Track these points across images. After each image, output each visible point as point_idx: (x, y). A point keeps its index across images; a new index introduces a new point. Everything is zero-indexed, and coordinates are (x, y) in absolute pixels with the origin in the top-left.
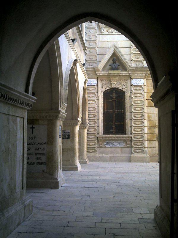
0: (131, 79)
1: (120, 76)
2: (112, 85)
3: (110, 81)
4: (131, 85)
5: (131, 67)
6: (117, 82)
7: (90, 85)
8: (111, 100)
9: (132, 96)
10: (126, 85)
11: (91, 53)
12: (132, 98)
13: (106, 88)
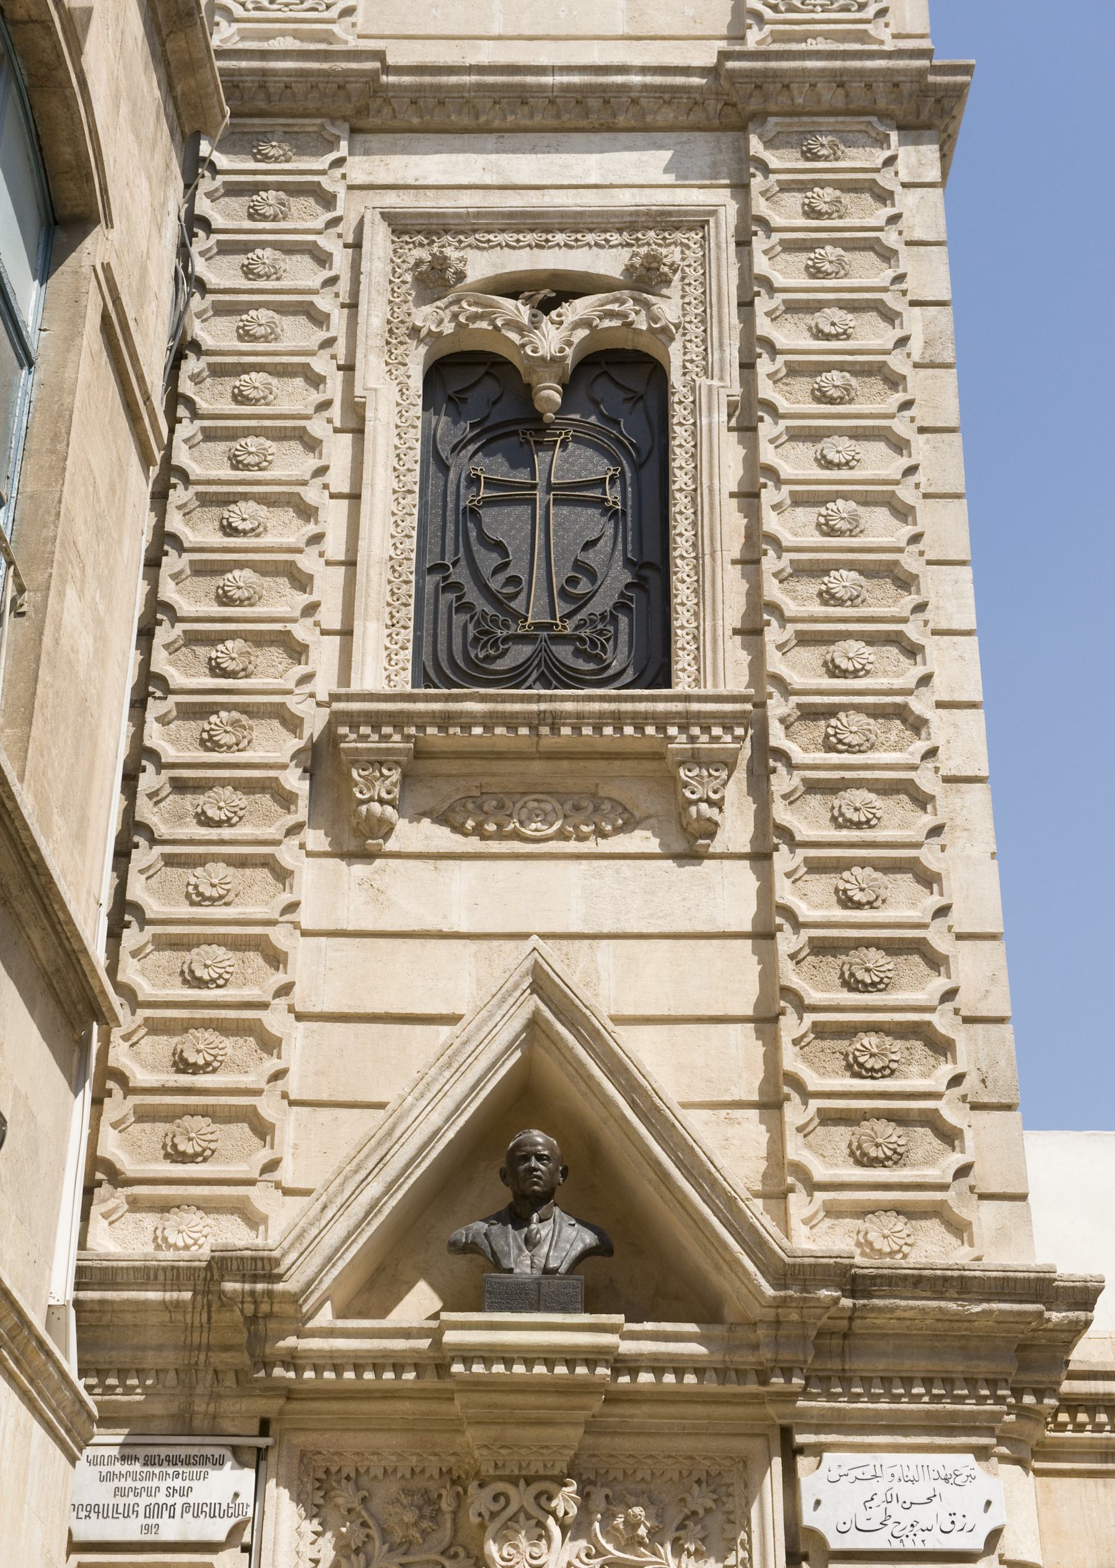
11: (185, 1080)
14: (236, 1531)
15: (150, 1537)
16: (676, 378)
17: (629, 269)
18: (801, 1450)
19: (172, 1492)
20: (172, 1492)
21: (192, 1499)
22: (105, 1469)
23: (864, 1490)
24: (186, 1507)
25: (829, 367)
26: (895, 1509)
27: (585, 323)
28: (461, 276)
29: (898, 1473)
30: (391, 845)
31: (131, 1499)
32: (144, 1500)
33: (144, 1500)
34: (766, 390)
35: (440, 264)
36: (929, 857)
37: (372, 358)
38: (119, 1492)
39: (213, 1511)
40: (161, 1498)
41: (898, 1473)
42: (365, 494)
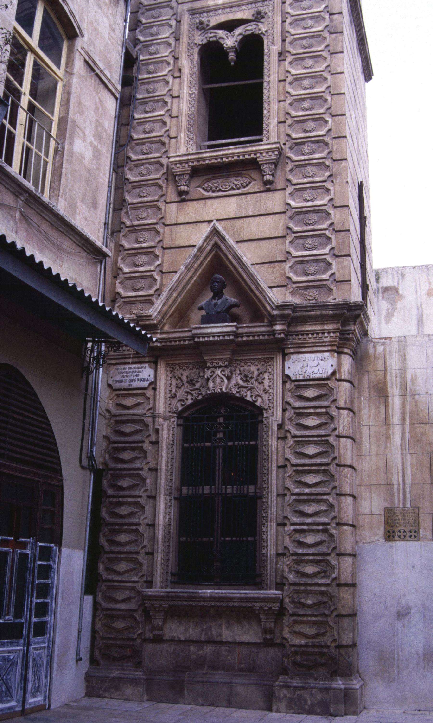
2: (211, 384)
3: (203, 366)
4: (284, 382)
5: (278, 307)
6: (227, 372)
7: (125, 385)
8: (207, 444)
9: (288, 426)
10: (266, 382)
12: (288, 431)
13: (189, 397)
14: (150, 384)
15: (131, 387)
16: (265, 46)
17: (253, 15)
18: (287, 354)
19: (135, 376)
20: (135, 376)
21: (139, 377)
22: (119, 371)
23: (301, 364)
24: (138, 380)
25: (305, 38)
26: (309, 369)
27: (241, 34)
28: (208, 25)
30: (187, 198)
31: (125, 378)
32: (128, 379)
33: (128, 379)
34: (288, 47)
35: (201, 23)
36: (328, 185)
39: (144, 380)
40: (132, 378)
42: (181, 96)
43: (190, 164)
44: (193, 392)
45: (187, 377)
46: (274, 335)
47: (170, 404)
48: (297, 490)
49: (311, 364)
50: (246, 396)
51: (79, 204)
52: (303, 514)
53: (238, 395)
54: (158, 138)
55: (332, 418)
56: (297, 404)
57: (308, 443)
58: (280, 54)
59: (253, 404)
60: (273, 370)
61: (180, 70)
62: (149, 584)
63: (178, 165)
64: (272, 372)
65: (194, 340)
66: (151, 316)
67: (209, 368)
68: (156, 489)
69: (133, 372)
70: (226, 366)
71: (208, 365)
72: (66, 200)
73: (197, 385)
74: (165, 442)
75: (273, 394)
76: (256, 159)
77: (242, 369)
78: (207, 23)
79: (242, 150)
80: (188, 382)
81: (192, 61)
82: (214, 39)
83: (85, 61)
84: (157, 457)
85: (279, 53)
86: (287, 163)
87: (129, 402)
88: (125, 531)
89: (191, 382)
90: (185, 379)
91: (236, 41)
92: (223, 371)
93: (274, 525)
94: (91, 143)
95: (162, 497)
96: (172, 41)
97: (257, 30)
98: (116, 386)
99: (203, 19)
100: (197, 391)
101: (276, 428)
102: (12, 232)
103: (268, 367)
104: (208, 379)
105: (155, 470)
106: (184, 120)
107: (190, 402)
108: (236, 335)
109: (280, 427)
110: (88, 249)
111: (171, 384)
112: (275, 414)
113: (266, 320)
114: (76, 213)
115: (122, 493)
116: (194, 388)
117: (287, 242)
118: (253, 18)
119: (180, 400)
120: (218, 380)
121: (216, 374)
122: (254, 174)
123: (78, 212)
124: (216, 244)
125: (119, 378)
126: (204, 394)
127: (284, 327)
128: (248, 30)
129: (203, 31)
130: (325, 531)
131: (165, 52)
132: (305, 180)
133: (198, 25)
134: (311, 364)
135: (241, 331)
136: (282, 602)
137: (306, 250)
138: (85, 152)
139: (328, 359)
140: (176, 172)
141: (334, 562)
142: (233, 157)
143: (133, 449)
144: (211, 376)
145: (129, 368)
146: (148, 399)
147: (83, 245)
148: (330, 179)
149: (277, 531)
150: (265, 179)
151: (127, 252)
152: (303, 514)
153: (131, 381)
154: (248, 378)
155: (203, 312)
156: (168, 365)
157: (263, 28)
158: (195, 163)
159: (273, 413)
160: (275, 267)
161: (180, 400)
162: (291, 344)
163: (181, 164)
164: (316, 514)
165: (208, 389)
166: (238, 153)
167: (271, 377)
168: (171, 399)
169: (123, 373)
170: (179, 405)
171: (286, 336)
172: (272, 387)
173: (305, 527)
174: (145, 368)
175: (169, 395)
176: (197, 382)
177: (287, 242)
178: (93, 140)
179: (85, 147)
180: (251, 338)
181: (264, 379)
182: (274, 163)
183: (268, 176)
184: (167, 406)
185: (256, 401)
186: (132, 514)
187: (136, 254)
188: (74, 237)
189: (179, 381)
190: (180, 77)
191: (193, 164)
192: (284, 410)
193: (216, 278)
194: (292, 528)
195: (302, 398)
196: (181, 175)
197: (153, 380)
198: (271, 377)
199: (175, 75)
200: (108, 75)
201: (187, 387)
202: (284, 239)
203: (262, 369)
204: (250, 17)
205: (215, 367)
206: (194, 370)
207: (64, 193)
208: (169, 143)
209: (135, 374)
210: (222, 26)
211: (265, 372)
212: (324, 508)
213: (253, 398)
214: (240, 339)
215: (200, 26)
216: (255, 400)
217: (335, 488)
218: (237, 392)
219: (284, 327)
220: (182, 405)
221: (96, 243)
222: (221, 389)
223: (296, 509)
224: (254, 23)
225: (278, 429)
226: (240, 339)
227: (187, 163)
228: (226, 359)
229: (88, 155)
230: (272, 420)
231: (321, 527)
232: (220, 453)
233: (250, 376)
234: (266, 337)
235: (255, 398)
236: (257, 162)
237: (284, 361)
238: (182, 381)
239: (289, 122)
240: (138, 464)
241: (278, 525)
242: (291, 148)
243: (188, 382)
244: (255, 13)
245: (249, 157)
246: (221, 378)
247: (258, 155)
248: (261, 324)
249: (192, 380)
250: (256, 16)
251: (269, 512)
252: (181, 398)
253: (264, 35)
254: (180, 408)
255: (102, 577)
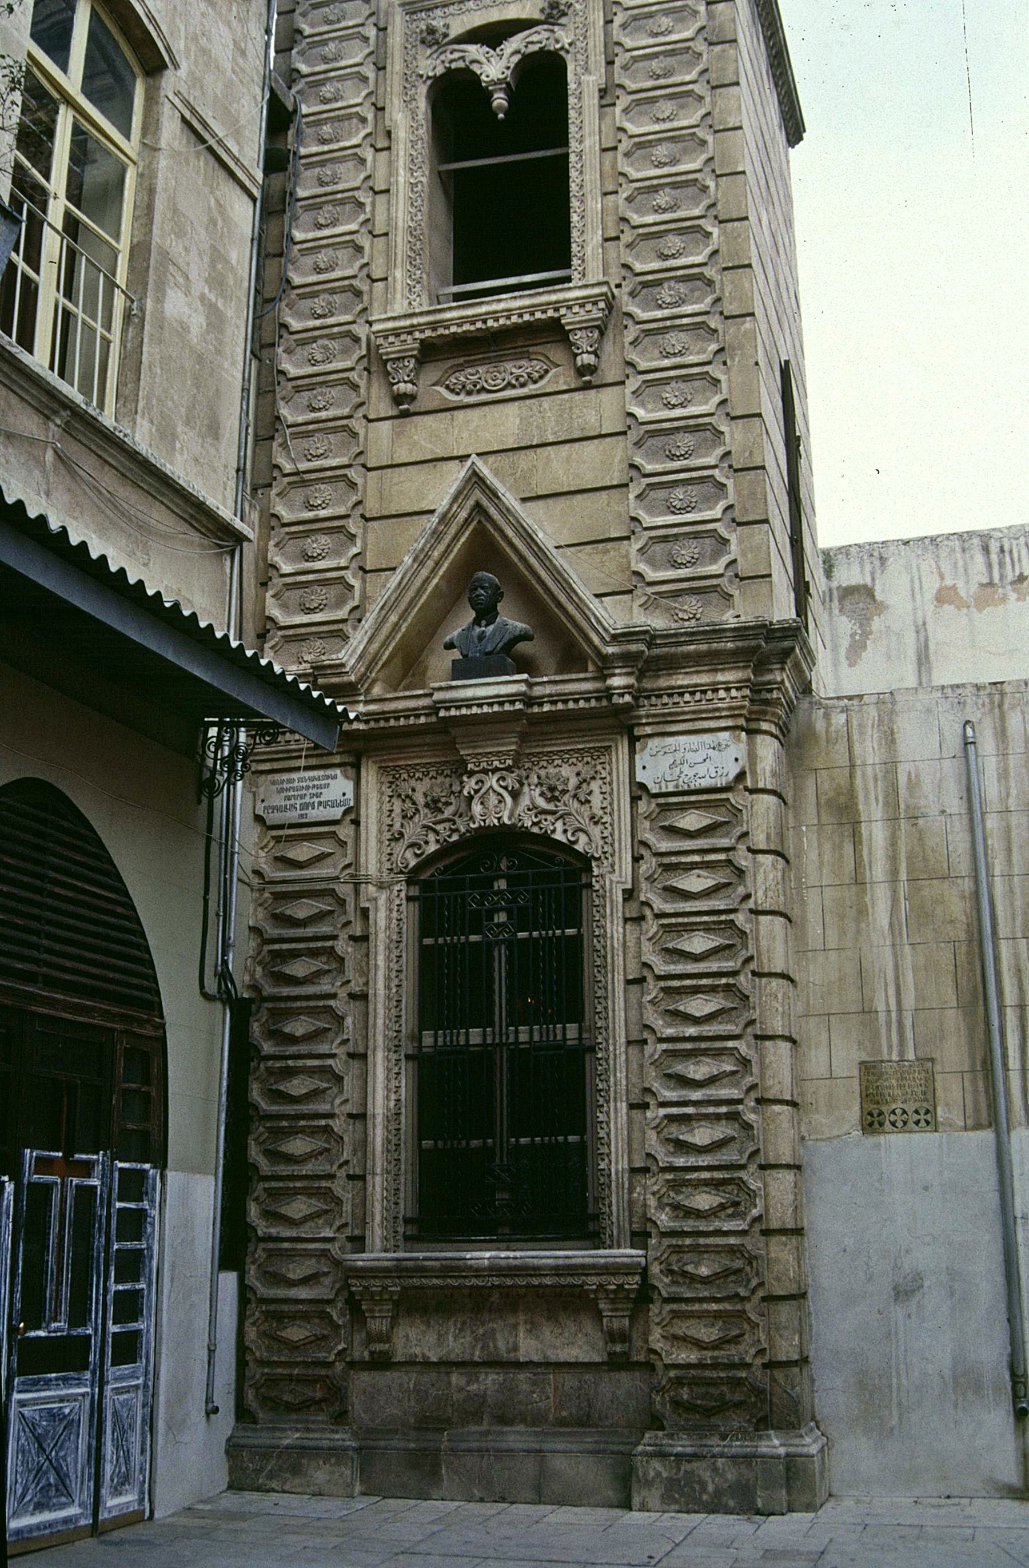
0: (633, 740)
1: (538, 721)
2: (477, 808)
3: (460, 769)
4: (634, 799)
5: (615, 637)
6: (511, 781)
7: (293, 816)
8: (473, 938)
10: (596, 800)
12: (647, 904)
13: (432, 837)
14: (346, 813)
16: (570, 77)
17: (542, 10)
18: (638, 738)
19: (313, 796)
20: (313, 796)
24: (320, 803)
25: (656, 55)
26: (685, 768)
27: (517, 52)
28: (445, 35)
29: (688, 747)
30: (412, 408)
31: (292, 802)
32: (299, 802)
33: (299, 802)
35: (431, 31)
36: (715, 371)
37: (396, 101)
38: (288, 798)
39: (334, 804)
40: (307, 800)
41: (688, 747)
42: (393, 189)
43: (417, 335)
44: (438, 827)
45: (425, 795)
46: (609, 697)
47: (390, 854)
48: (670, 1032)
49: (691, 757)
50: (554, 831)
51: (180, 429)
52: (685, 1082)
53: (535, 830)
54: (346, 282)
55: (740, 873)
56: (665, 845)
57: (690, 928)
58: (603, 92)
59: (567, 848)
60: (610, 774)
61: (389, 134)
62: (359, 1242)
63: (391, 339)
64: (608, 779)
65: (437, 714)
66: (343, 665)
67: (471, 774)
68: (366, 1037)
69: (308, 788)
70: (509, 769)
71: (470, 766)
72: (152, 422)
73: (448, 812)
74: (381, 936)
75: (612, 825)
76: (559, 319)
77: (543, 772)
78: (444, 30)
79: (527, 302)
80: (427, 805)
81: (414, 114)
82: (461, 64)
83: (184, 119)
84: (366, 971)
85: (600, 90)
86: (626, 327)
87: (302, 852)
88: (302, 1130)
89: (434, 805)
90: (420, 799)
91: (508, 68)
92: (503, 779)
93: (623, 1107)
94: (202, 298)
95: (380, 1055)
96: (369, 72)
97: (552, 41)
98: (273, 818)
99: (434, 23)
100: (447, 825)
101: (620, 900)
102: (39, 494)
103: (599, 767)
104: (470, 798)
105: (362, 997)
106: (401, 242)
107: (432, 848)
108: (529, 701)
109: (629, 895)
110: (204, 526)
111: (391, 811)
112: (616, 867)
113: (591, 668)
114: (174, 449)
115: (293, 1049)
116: (440, 817)
117: (631, 496)
118: (543, 17)
119: (412, 845)
120: (493, 799)
121: (487, 786)
122: (556, 353)
123: (178, 446)
124: (478, 506)
125: (278, 801)
126: (463, 830)
127: (631, 680)
128: (532, 43)
129: (435, 47)
130: (733, 1117)
131: (354, 96)
132: (666, 363)
133: (425, 34)
134: (691, 757)
135: (538, 691)
136: (645, 1272)
137: (673, 513)
138: (190, 316)
139: (727, 746)
140: (387, 354)
141: (754, 1184)
142: (508, 318)
143: (314, 953)
144: (476, 791)
145: (300, 780)
146: (343, 844)
147: (192, 516)
148: (720, 358)
149: (630, 1122)
150: (579, 363)
151: (287, 529)
152: (685, 1082)
153: (305, 806)
154: (557, 794)
155: (456, 654)
156: (383, 770)
157: (565, 37)
158: (428, 333)
159: (612, 866)
160: (606, 552)
161: (412, 845)
162: (648, 716)
163: (398, 335)
164: (711, 1081)
165: (472, 819)
166: (520, 308)
167: (606, 788)
168: (393, 844)
169: (287, 790)
170: (409, 854)
171: (636, 698)
172: (608, 810)
173: (690, 1110)
174: (335, 777)
175: (388, 836)
176: (448, 804)
177: (631, 496)
178: (206, 291)
179: (189, 305)
180: (560, 706)
181: (590, 793)
182: (597, 327)
183: (585, 356)
184: (385, 859)
185: (576, 842)
186: (315, 1094)
187: (307, 534)
188: (172, 501)
189: (408, 804)
190: (389, 148)
191: (423, 336)
192: (636, 859)
193: (480, 580)
194: (662, 1112)
195: (673, 831)
196: (398, 359)
197: (352, 804)
198: (606, 788)
199: (379, 146)
200: (235, 150)
201: (425, 817)
202: (624, 489)
203: (587, 772)
204: (537, 16)
205: (485, 772)
206: (440, 779)
207: (148, 407)
208: (371, 291)
209: (314, 791)
210: (474, 36)
211: (593, 778)
212: (729, 1068)
213: (569, 834)
214: (536, 709)
215: (429, 38)
216: (572, 839)
217: (752, 1022)
218: (534, 824)
219: (631, 680)
220: (417, 855)
221: (220, 513)
222: (499, 819)
223: (669, 1071)
224: (545, 27)
225: (625, 900)
226: (536, 709)
227: (410, 333)
228: (506, 753)
229: (197, 322)
230: (611, 881)
231: (724, 1109)
232: (500, 955)
233: (560, 788)
234: (593, 703)
235: (573, 834)
236: (562, 326)
237: (632, 752)
238: (414, 803)
239: (627, 237)
240: (325, 986)
241: (632, 1106)
242: (632, 294)
243: (427, 805)
244: (546, 5)
245: (544, 316)
246: (499, 794)
247: (563, 311)
248: (582, 676)
249: (436, 801)
250: (548, 11)
251: (612, 1079)
252: (413, 840)
253: (568, 52)
254: (413, 863)
255: (255, 1230)
